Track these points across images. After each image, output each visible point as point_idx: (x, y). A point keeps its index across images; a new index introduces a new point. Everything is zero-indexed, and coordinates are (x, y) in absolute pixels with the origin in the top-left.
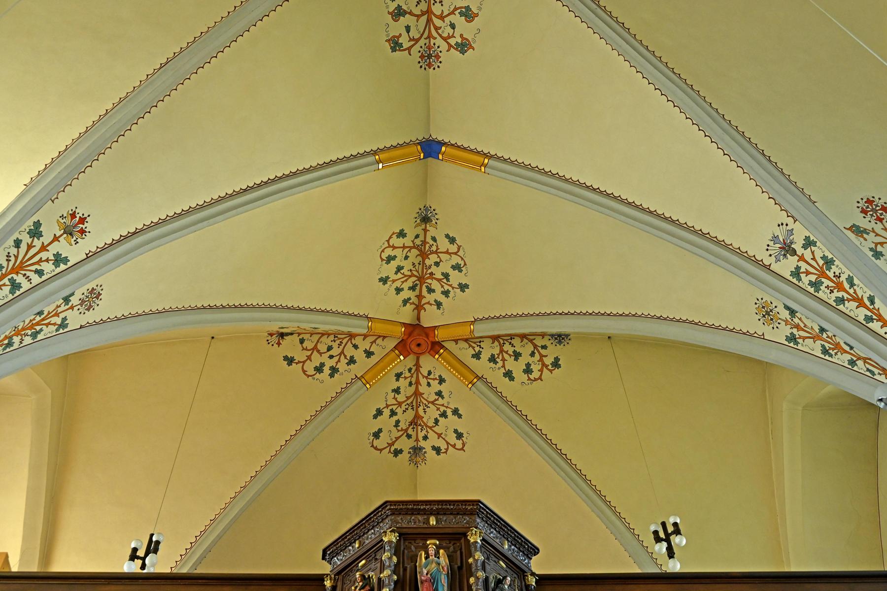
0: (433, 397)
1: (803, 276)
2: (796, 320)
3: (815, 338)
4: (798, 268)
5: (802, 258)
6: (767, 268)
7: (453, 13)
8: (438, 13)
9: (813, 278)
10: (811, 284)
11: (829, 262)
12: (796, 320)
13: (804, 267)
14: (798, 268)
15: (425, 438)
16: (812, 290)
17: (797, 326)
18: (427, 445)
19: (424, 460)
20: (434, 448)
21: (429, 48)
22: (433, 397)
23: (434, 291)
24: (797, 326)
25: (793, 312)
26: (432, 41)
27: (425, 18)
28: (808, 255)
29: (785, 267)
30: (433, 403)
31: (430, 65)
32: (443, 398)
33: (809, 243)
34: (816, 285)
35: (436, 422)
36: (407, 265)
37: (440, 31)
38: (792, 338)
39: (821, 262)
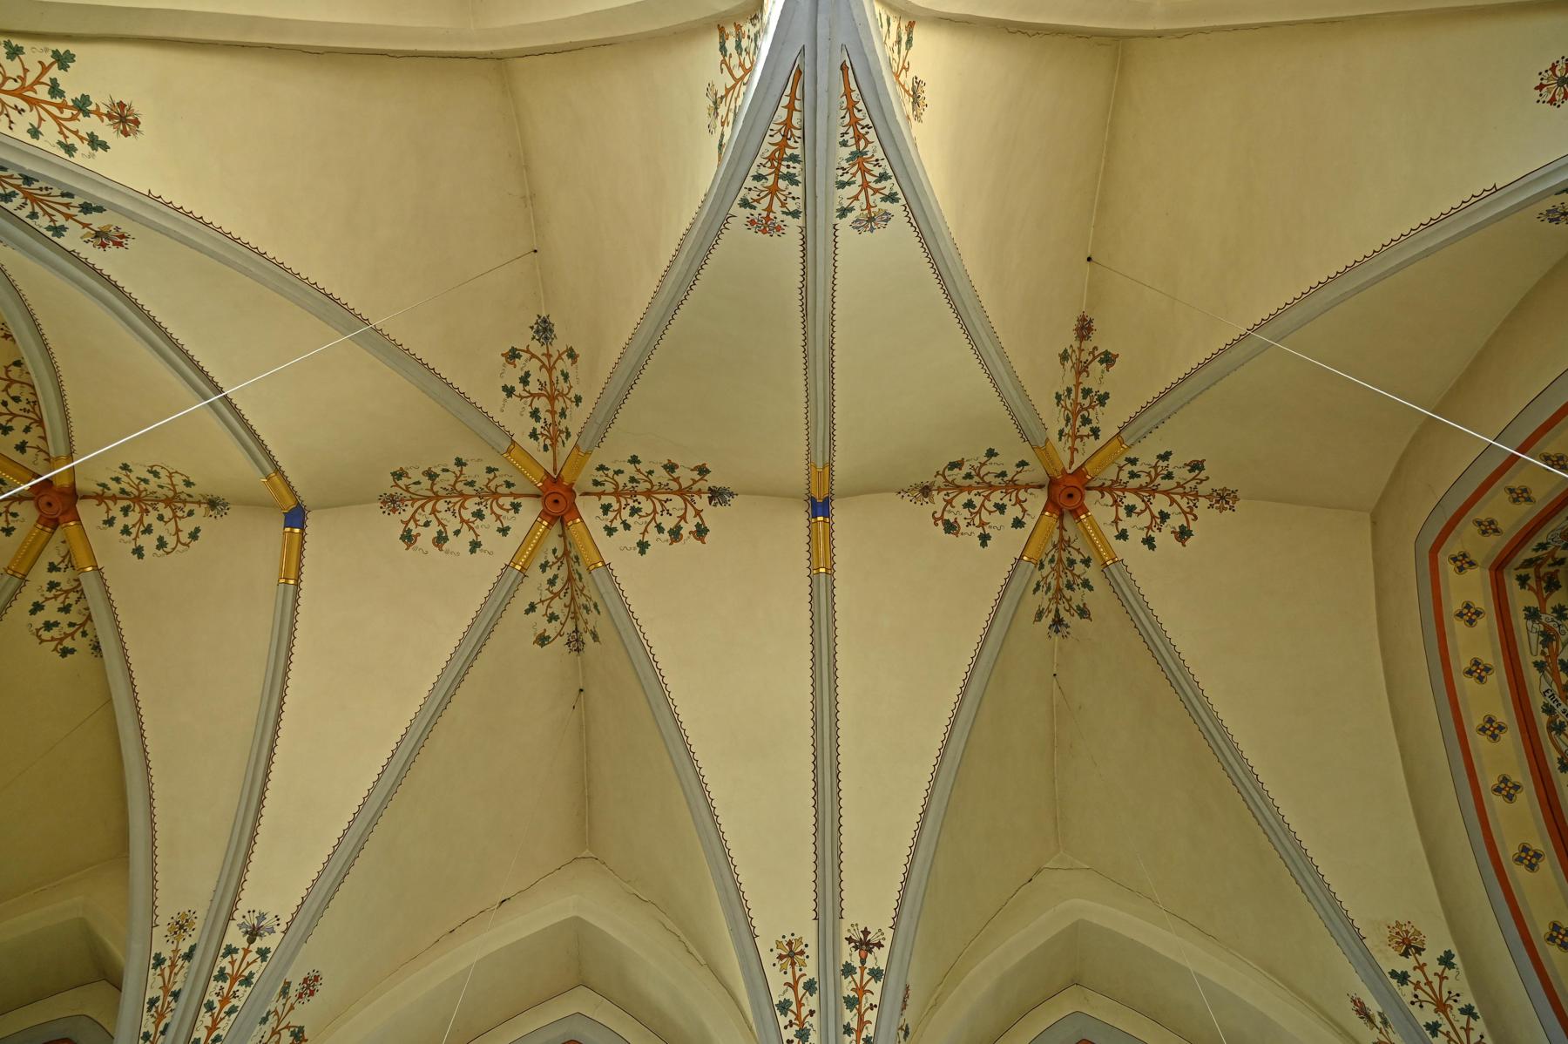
1: (229, 958)
2: (180, 962)
3: (164, 987)
4: (236, 951)
5: (247, 951)
6: (230, 917)
9: (228, 970)
10: (222, 970)
11: (247, 981)
12: (180, 962)
13: (238, 957)
14: (236, 951)
16: (216, 973)
17: (173, 965)
23: (126, 515)
24: (173, 965)
25: (188, 957)
28: (253, 956)
29: (235, 937)
33: (263, 953)
34: (222, 976)
38: (159, 961)
39: (246, 973)
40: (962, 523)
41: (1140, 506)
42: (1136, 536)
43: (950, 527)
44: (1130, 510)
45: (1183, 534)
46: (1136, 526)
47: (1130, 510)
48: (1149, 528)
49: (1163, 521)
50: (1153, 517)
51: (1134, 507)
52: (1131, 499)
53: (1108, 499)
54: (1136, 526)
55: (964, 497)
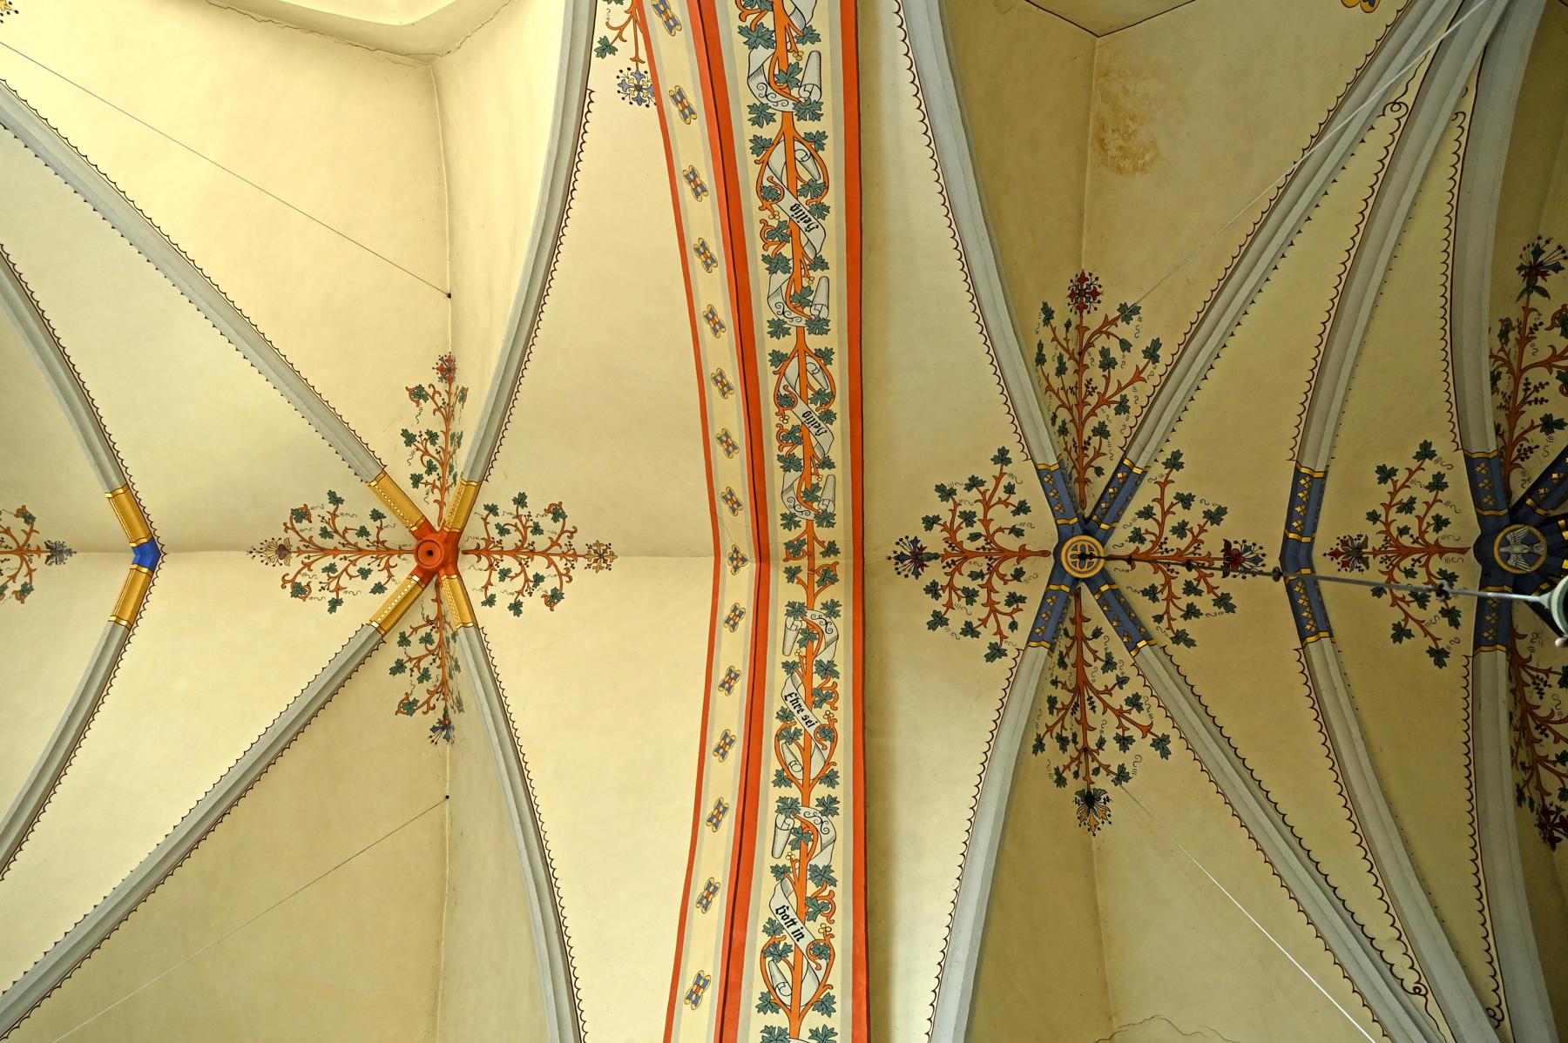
40: (315, 586)
41: (516, 569)
42: (503, 601)
43: (299, 591)
44: (504, 574)
45: (554, 598)
46: (505, 592)
47: (504, 574)
48: (520, 593)
49: (536, 585)
50: (527, 580)
51: (509, 570)
52: (508, 562)
53: (484, 563)
54: (505, 592)
55: (327, 561)
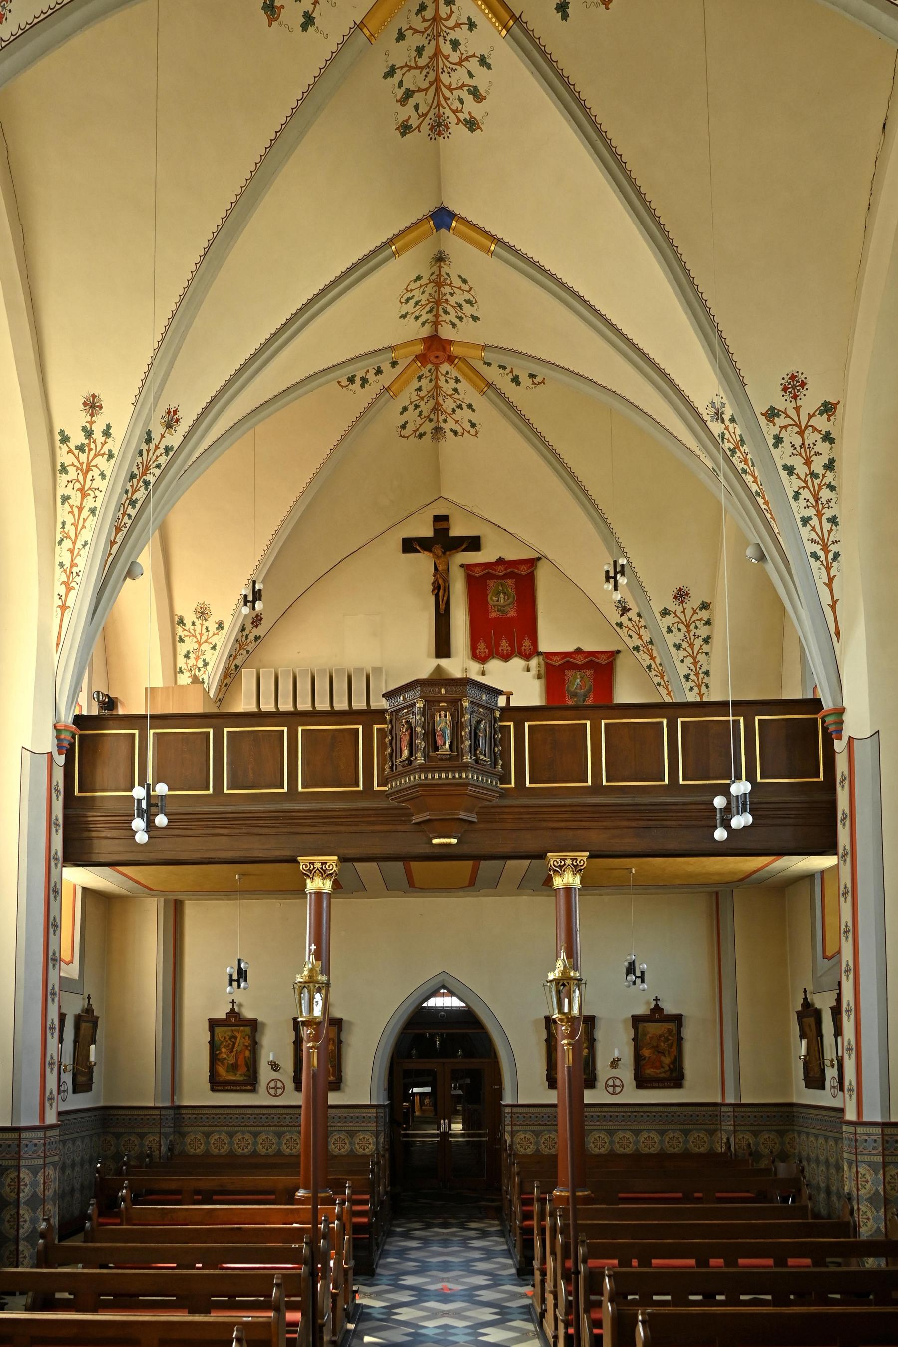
0: (451, 392)
7: (461, 88)
8: (447, 84)
15: (445, 421)
18: (447, 427)
19: (444, 437)
20: (452, 430)
21: (439, 116)
22: (451, 392)
26: (441, 110)
27: (433, 88)
30: (450, 396)
31: (439, 134)
32: (459, 394)
35: (454, 411)
36: (424, 299)
37: (449, 102)
